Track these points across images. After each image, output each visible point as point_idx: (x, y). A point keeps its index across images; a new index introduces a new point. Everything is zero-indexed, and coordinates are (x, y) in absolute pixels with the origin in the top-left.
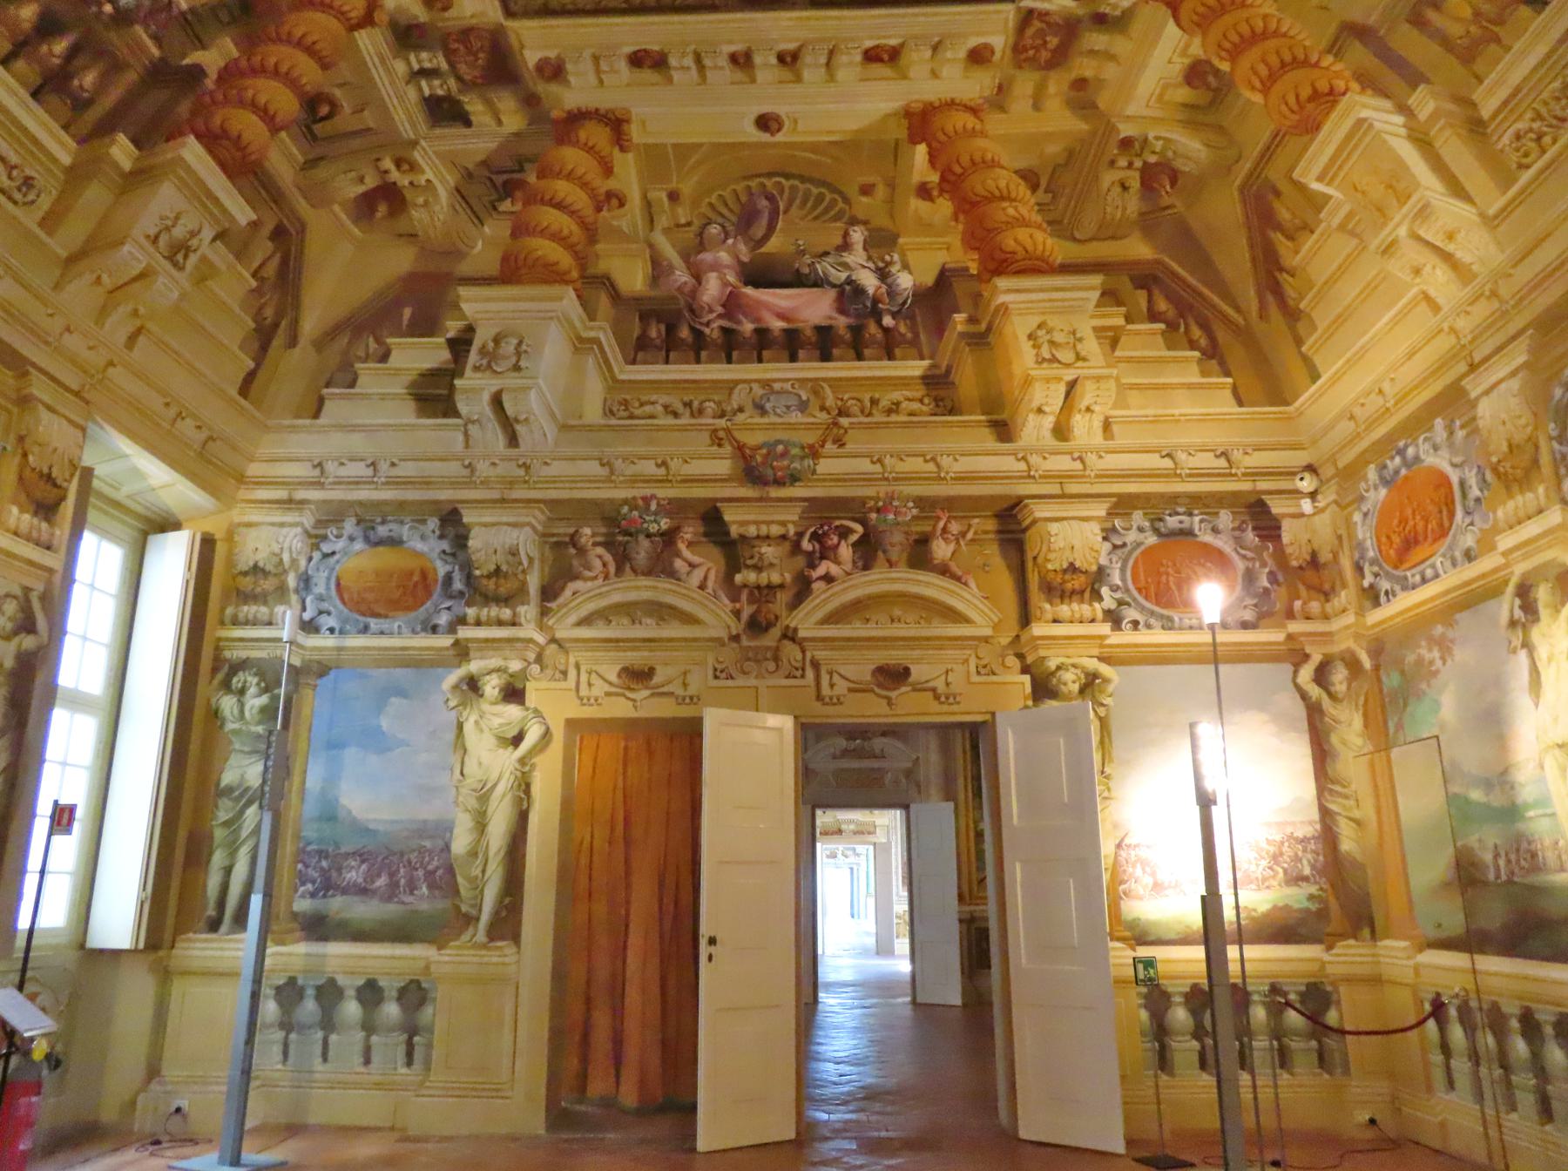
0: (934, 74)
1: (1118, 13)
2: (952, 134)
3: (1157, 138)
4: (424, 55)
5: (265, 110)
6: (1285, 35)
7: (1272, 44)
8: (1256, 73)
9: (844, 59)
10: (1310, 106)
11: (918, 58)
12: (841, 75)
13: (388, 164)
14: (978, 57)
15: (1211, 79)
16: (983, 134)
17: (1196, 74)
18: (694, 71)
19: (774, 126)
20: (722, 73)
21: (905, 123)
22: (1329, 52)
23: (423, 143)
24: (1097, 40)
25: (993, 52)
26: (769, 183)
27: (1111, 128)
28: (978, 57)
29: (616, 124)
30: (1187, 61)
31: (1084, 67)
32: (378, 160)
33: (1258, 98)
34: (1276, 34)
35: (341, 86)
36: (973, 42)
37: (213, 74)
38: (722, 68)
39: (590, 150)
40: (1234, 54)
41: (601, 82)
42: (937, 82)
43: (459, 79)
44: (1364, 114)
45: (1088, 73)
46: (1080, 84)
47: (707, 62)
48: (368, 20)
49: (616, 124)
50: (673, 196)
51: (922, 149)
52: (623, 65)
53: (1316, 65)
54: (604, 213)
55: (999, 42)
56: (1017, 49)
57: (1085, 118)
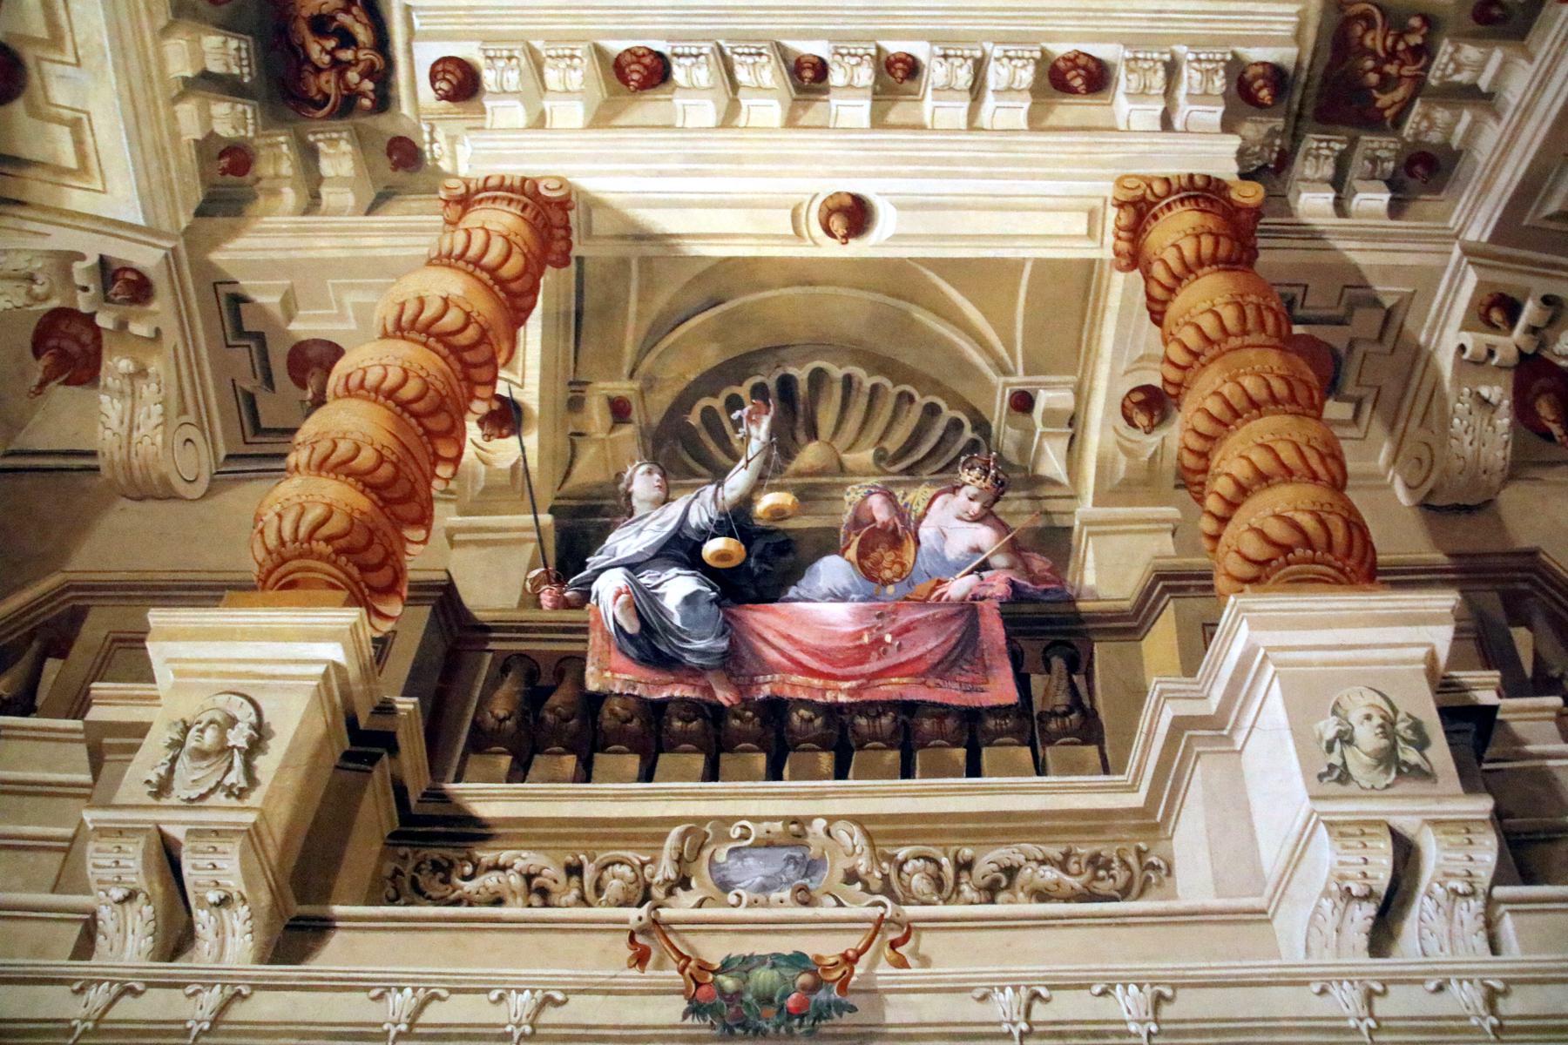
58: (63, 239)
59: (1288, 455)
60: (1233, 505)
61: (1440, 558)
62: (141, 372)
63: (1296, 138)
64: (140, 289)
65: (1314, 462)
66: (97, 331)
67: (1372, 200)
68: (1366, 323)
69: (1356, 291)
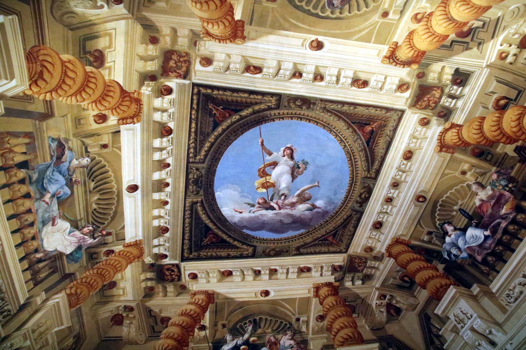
0: (229, 56)
1: (146, 83)
2: (220, 23)
3: (102, 7)
4: (447, 104)
5: (519, 119)
6: (71, 96)
7: (75, 88)
8: (72, 71)
9: (271, 71)
10: (39, 69)
11: (237, 64)
12: (274, 64)
13: (510, 59)
14: (207, 61)
15: (92, 59)
16: (202, 19)
17: (99, 59)
18: (343, 74)
19: (315, 44)
20: (330, 74)
21: (245, 34)
22: (50, 101)
23: (484, 65)
24: (152, 66)
25: (200, 62)
26: (328, 13)
27: (130, 10)
28: (207, 61)
29: (392, 57)
30: (107, 65)
31: (152, 50)
32: (511, 64)
33: (65, 57)
34: (75, 94)
35: (487, 108)
36: (210, 68)
37: (514, 146)
38: (329, 75)
39: (412, 46)
40: (87, 78)
41: (385, 78)
42: (228, 53)
43: (442, 91)
44: (14, 83)
45: (151, 47)
46: (154, 41)
47: (334, 79)
48: (453, 126)
49: (392, 57)
50: (385, 14)
51: (238, 16)
52: (372, 83)
53: (51, 92)
54: (429, 11)
55: (197, 67)
56: (188, 62)
57: (146, 19)
58: (118, 304)
59: (346, 323)
60: (337, 333)
61: (375, 338)
62: (131, 323)
63: (345, 275)
64: (131, 309)
65: (351, 324)
66: (123, 317)
67: (359, 283)
68: (359, 301)
69: (357, 297)
